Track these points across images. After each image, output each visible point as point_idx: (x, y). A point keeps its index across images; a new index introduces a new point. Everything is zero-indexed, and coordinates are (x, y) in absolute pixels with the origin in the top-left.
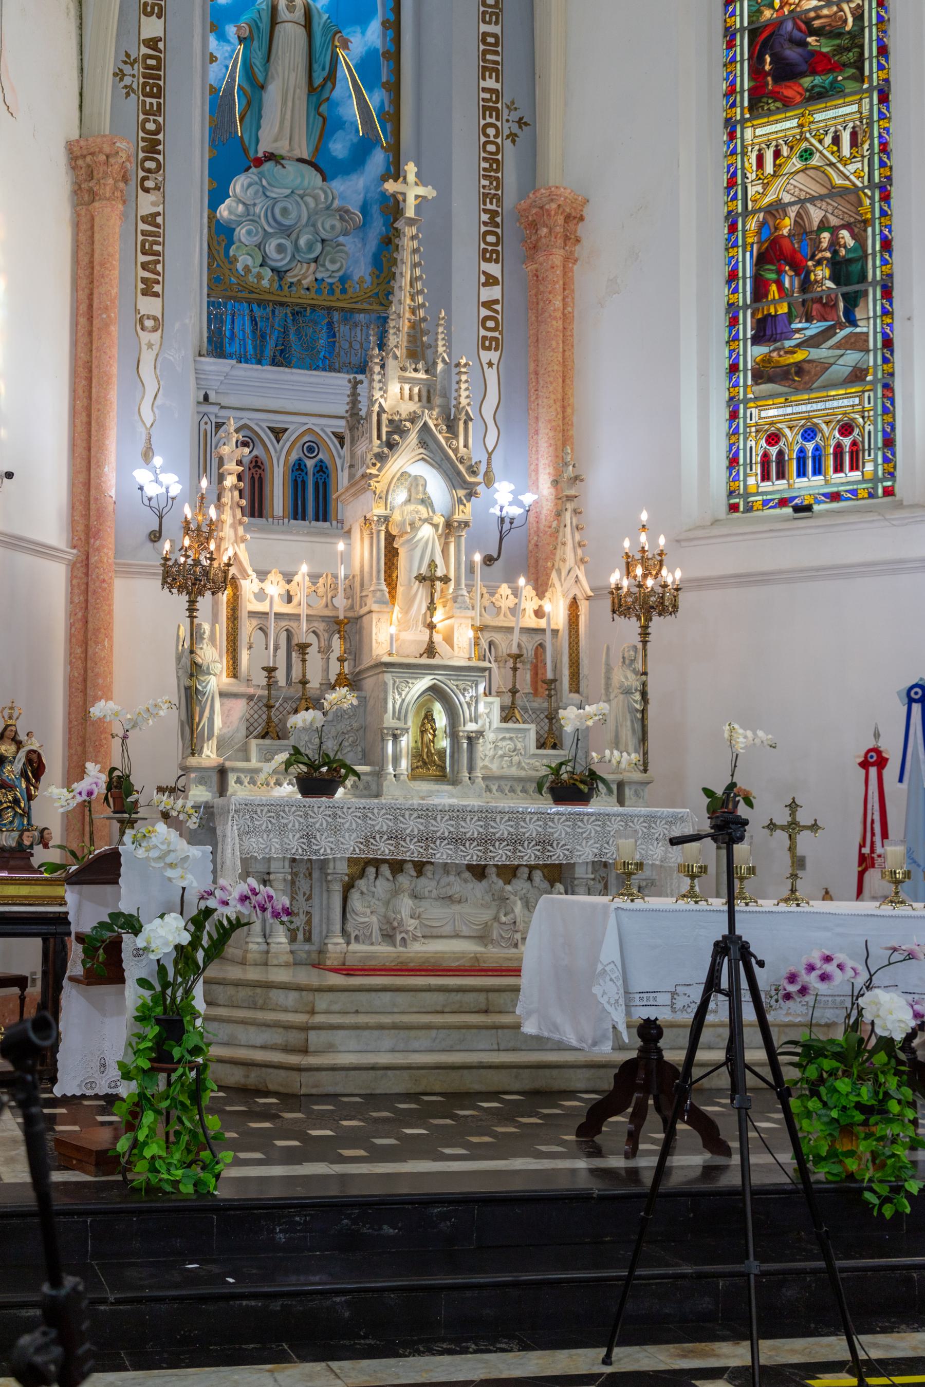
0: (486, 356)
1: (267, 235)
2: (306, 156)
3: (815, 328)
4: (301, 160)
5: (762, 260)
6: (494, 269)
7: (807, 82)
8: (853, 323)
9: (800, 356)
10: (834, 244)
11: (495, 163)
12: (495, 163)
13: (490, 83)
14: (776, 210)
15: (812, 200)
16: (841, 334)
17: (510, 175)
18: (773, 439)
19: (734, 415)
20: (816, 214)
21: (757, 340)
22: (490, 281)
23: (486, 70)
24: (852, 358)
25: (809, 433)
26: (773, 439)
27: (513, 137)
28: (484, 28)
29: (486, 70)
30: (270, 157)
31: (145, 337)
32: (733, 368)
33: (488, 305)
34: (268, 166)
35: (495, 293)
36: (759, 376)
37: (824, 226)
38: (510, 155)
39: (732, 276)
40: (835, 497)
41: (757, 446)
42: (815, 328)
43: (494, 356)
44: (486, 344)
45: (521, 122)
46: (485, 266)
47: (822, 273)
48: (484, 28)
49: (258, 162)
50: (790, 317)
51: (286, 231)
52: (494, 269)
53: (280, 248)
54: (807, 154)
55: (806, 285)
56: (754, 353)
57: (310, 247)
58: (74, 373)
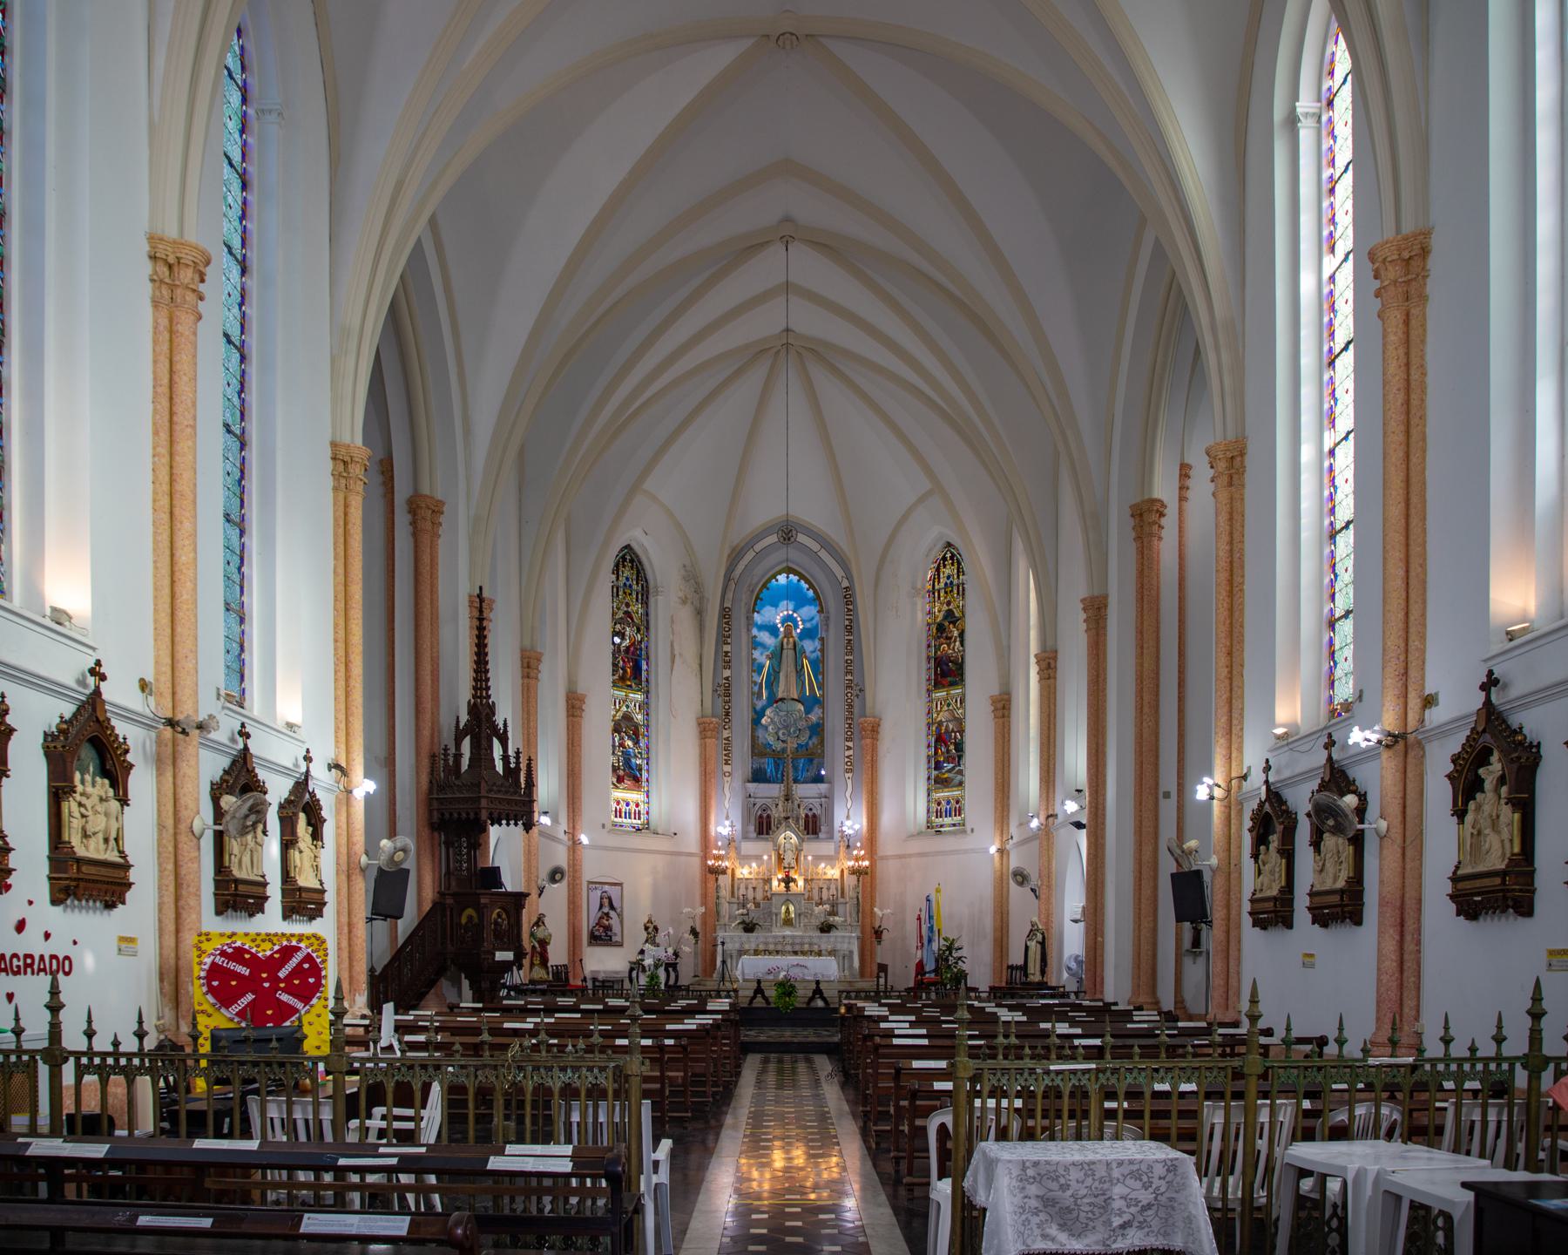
0: (847, 775)
1: (779, 729)
2: (796, 697)
3: (951, 765)
4: (793, 699)
5: (936, 741)
6: (850, 744)
7: (949, 679)
8: (959, 765)
9: (946, 776)
10: (955, 736)
11: (850, 706)
12: (850, 706)
13: (849, 677)
14: (940, 723)
15: (950, 721)
16: (957, 768)
17: (856, 710)
18: (939, 804)
19: (929, 795)
20: (951, 726)
21: (936, 769)
22: (849, 748)
23: (848, 672)
24: (959, 777)
25: (948, 803)
26: (939, 804)
27: (857, 696)
28: (847, 658)
29: (848, 672)
30: (782, 700)
31: (726, 779)
32: (929, 778)
33: (848, 757)
34: (780, 703)
35: (851, 752)
36: (936, 782)
37: (953, 731)
38: (857, 702)
39: (929, 746)
40: (954, 825)
41: (934, 806)
42: (951, 765)
43: (850, 775)
44: (847, 771)
45: (861, 690)
46: (847, 743)
47: (952, 747)
48: (847, 658)
49: (777, 702)
50: (944, 762)
51: (786, 727)
52: (850, 744)
53: (783, 734)
54: (949, 705)
55: (948, 751)
56: (934, 773)
57: (795, 732)
58: (701, 795)
